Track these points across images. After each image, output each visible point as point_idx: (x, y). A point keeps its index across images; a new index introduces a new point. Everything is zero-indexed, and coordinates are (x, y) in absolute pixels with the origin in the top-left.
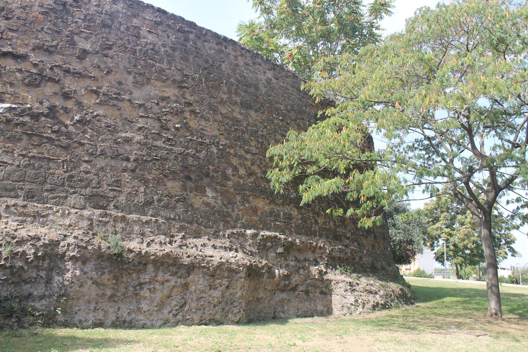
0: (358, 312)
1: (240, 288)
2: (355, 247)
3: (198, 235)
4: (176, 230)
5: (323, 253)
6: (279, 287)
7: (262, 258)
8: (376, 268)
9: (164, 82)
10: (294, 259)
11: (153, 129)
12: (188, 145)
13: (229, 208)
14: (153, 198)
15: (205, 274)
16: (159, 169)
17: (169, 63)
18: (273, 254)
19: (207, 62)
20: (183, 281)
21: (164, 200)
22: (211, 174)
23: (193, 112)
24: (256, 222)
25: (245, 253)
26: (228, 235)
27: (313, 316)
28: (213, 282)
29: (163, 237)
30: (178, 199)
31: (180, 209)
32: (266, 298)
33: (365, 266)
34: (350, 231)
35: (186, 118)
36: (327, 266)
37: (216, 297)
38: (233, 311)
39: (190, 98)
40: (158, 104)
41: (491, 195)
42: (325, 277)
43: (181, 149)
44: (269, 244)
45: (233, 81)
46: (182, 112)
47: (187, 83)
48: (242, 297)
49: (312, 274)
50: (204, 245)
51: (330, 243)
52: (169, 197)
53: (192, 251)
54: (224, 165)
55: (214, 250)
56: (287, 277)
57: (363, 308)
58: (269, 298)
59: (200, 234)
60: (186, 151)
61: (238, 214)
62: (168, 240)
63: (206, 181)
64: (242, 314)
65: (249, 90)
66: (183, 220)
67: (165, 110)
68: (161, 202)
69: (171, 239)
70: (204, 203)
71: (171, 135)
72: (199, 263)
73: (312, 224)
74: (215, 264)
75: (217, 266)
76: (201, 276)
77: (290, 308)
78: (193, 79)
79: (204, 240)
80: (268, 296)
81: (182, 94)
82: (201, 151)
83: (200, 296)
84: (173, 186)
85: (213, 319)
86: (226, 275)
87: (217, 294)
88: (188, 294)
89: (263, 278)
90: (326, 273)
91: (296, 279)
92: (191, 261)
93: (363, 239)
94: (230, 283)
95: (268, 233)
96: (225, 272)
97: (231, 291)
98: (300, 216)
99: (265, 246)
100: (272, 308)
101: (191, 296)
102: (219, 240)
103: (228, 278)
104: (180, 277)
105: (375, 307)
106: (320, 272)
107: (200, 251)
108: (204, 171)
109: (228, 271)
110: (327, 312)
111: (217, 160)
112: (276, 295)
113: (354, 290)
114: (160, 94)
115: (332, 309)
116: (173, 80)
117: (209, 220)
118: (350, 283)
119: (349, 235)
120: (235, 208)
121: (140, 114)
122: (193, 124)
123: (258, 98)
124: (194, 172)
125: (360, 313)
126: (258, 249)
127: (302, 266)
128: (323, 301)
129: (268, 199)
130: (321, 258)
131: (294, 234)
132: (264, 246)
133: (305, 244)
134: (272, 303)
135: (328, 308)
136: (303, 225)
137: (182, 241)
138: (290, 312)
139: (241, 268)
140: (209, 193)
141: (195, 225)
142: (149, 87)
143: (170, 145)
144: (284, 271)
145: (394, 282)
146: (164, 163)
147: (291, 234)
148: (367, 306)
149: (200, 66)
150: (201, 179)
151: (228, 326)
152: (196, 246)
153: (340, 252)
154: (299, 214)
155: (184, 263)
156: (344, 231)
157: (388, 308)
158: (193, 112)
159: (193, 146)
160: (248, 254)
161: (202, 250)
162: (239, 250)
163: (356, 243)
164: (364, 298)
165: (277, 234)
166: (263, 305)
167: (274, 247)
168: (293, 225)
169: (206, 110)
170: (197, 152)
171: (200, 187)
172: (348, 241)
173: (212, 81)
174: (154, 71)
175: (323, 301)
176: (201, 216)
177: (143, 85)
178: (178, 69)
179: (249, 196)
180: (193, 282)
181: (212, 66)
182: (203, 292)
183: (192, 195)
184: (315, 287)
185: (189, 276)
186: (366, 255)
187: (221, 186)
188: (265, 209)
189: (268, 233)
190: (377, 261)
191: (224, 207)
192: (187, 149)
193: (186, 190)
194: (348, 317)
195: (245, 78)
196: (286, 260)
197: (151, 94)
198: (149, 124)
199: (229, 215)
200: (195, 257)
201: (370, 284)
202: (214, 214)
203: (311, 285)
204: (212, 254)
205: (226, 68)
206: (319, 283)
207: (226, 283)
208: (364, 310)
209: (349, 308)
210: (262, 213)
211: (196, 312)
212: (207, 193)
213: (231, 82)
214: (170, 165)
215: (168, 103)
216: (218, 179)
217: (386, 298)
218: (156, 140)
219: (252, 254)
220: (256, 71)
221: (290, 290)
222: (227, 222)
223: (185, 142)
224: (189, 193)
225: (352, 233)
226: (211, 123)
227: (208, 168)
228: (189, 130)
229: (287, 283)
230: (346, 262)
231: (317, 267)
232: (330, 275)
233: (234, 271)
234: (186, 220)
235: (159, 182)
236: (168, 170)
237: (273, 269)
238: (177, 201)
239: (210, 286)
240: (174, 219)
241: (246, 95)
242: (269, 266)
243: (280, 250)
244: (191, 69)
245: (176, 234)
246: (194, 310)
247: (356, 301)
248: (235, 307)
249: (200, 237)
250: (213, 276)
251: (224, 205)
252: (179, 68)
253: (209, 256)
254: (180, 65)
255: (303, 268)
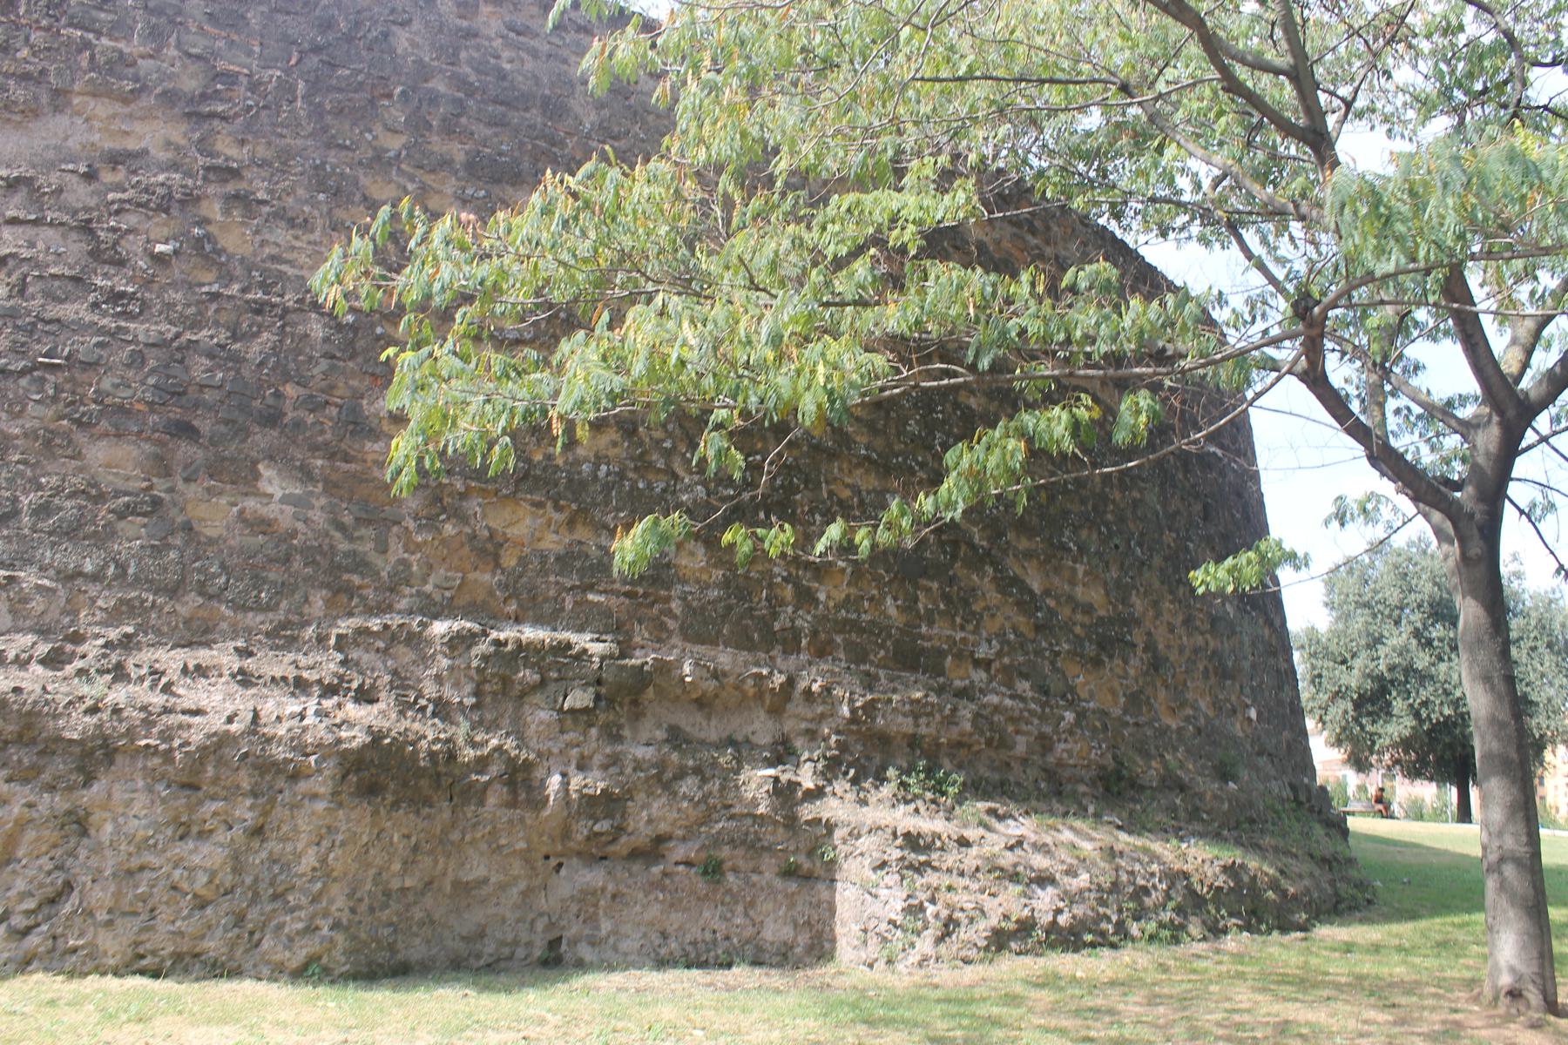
0: (914, 957)
1: (318, 837)
2: (1012, 697)
3: (198, 634)
4: (99, 615)
5: (822, 716)
6: (572, 844)
7: (491, 727)
8: (1133, 784)
9: (126, 101)
10: (660, 735)
11: (56, 264)
12: (200, 313)
13: (361, 538)
14: (15, 500)
15: (153, 777)
16: (55, 399)
17: (156, 35)
18: (544, 715)
19: (327, 25)
20: (60, 803)
21: (60, 509)
22: (290, 415)
23: (242, 200)
24: (491, 593)
25: (404, 707)
26: (339, 636)
27: (729, 966)
28: (192, 809)
29: (30, 638)
30: (127, 505)
31: (133, 538)
32: (503, 887)
33: (1067, 774)
34: (1001, 636)
35: (204, 222)
36: (832, 769)
37: (205, 870)
38: (280, 927)
39: (233, 152)
40: (90, 176)
41: (1489, 438)
42: (807, 812)
43: (164, 327)
44: (527, 675)
45: (442, 88)
46: (191, 199)
47: (230, 100)
48: (323, 870)
49: (740, 799)
50: (201, 671)
51: (869, 682)
52: (89, 497)
53: (120, 695)
54: (354, 383)
55: (236, 687)
56: (608, 804)
57: (940, 940)
58: (522, 885)
59: (206, 631)
60: (188, 336)
61: (403, 562)
62: (43, 649)
63: (263, 438)
64: (323, 937)
65: (515, 117)
66: (137, 579)
67: (119, 195)
68: (49, 516)
69: (69, 647)
70: (245, 521)
71: (131, 280)
72: (131, 733)
73: (783, 603)
74: (196, 738)
75: (203, 749)
76: (141, 784)
77: (626, 928)
78: (254, 87)
79: (223, 656)
80: (516, 878)
81: (201, 140)
82: (256, 335)
83: (135, 863)
84: (114, 461)
85: (197, 955)
86: (246, 785)
87: (208, 855)
88: (82, 853)
89: (482, 803)
90: (816, 794)
91: (650, 815)
92: (99, 726)
93: (1072, 669)
94: (265, 814)
95: (530, 633)
96: (242, 773)
97: (273, 845)
98: (718, 574)
99: (506, 682)
100: (540, 926)
101: (94, 862)
102: (291, 657)
103: (254, 794)
104: (51, 788)
105: (999, 941)
106: (784, 793)
107: (167, 689)
108: (257, 404)
109: (255, 767)
110: (810, 949)
111: (324, 364)
112: (563, 872)
113: (919, 869)
114: (108, 145)
115: (833, 941)
116: (164, 93)
117: (258, 581)
118: (907, 835)
119: (982, 652)
120: (392, 541)
121: (10, 213)
122: (236, 239)
123: (562, 144)
124: (210, 409)
125: (924, 959)
126: (477, 693)
127: (694, 760)
128: (792, 906)
129: (558, 508)
130: (812, 735)
131: (675, 640)
132: (502, 684)
133: (731, 680)
134: (542, 903)
135: (819, 936)
136: (729, 608)
137: (105, 656)
138: (624, 946)
139: (312, 759)
140: (273, 483)
141: (193, 600)
142: (63, 121)
143: (118, 315)
144: (596, 783)
145: (1216, 837)
146: (84, 377)
147: (660, 635)
148: (963, 934)
149: (293, 43)
150: (243, 433)
151: (248, 985)
152: (151, 674)
153: (916, 717)
154: (715, 566)
155: (67, 735)
156: (959, 635)
157: (1093, 945)
158: (242, 200)
159: (223, 318)
160: (423, 709)
161: (181, 691)
162: (383, 695)
163: (1024, 686)
164: (964, 900)
165: (583, 640)
166: (491, 911)
167: (552, 687)
168: (675, 605)
169: (301, 192)
170: (235, 338)
171: (233, 460)
172: (979, 676)
173: (340, 90)
174: (85, 64)
175: (792, 906)
176: (223, 566)
177: (35, 113)
178: (190, 56)
179: (463, 496)
180: (104, 808)
181: (349, 39)
182: (144, 845)
183: (193, 491)
184: (754, 847)
185: (87, 784)
186: (1071, 733)
187: (331, 457)
188: (544, 545)
189: (530, 633)
190: (1147, 755)
191: (337, 535)
192: (192, 327)
193: (167, 473)
194: (880, 973)
195: (504, 78)
196: (618, 738)
197: (70, 143)
198: (41, 245)
199: (360, 564)
200: (116, 711)
201: (1034, 845)
202: (287, 560)
203: (732, 841)
204: (203, 703)
205: (414, 45)
206: (776, 837)
207: (248, 815)
208: (942, 948)
209: (885, 940)
210: (523, 561)
211: (109, 924)
212: (264, 486)
213: (431, 91)
214: (106, 385)
215: (134, 172)
216: (322, 432)
217: (1102, 902)
218: (62, 301)
219: (442, 709)
220: (565, 53)
221: (635, 854)
222: (350, 591)
223: (189, 306)
224: (180, 485)
225: (1004, 641)
226: (316, 236)
227: (278, 395)
228: (214, 262)
229: (603, 826)
230: (952, 757)
231: (771, 772)
232: (833, 802)
233: (279, 771)
234: (147, 581)
235: (49, 443)
236: (95, 401)
237: (539, 773)
238: (121, 516)
239: (176, 822)
240: (96, 577)
241: (496, 135)
242: (511, 761)
243: (579, 698)
244: (250, 53)
245: (97, 630)
246: (102, 916)
247: (914, 910)
248: (292, 910)
249: (208, 645)
250: (184, 786)
251: (341, 527)
252: (194, 51)
253: (184, 712)
254: (203, 42)
255: (697, 771)
